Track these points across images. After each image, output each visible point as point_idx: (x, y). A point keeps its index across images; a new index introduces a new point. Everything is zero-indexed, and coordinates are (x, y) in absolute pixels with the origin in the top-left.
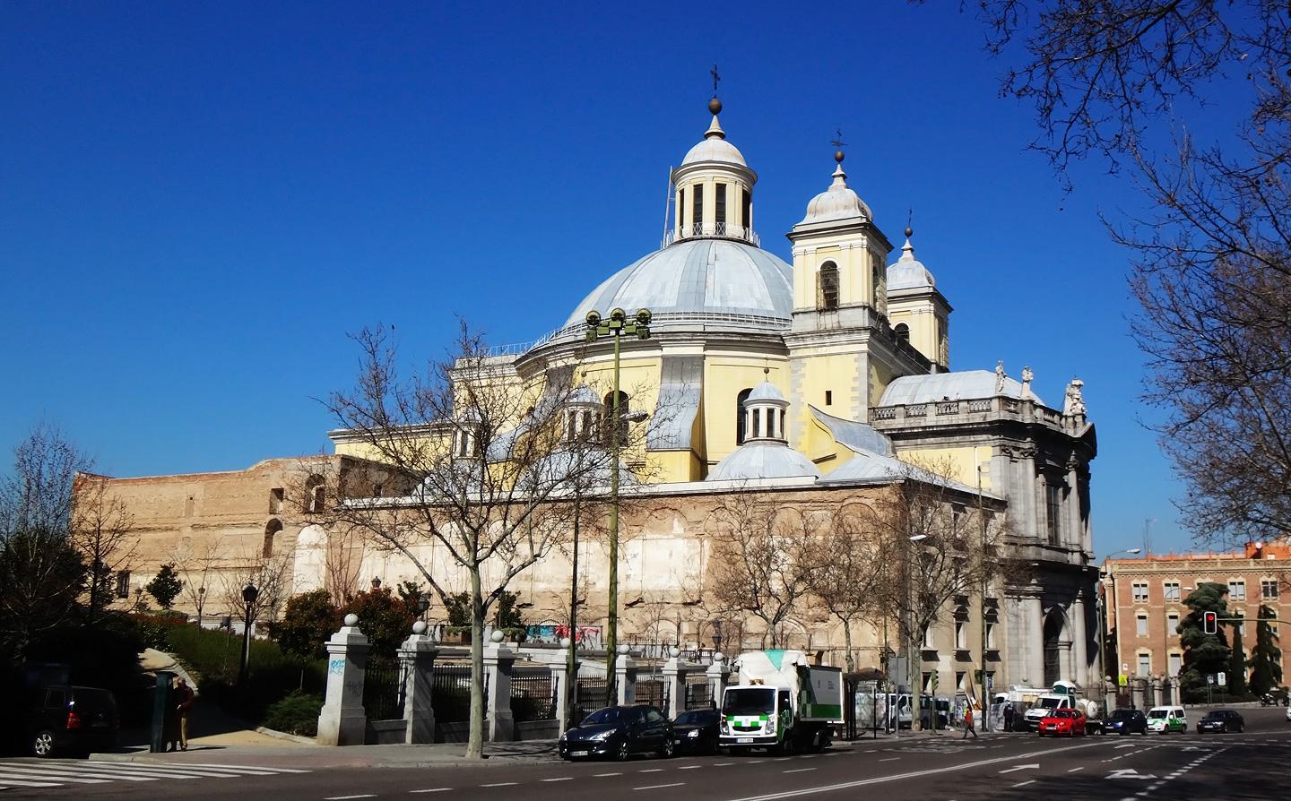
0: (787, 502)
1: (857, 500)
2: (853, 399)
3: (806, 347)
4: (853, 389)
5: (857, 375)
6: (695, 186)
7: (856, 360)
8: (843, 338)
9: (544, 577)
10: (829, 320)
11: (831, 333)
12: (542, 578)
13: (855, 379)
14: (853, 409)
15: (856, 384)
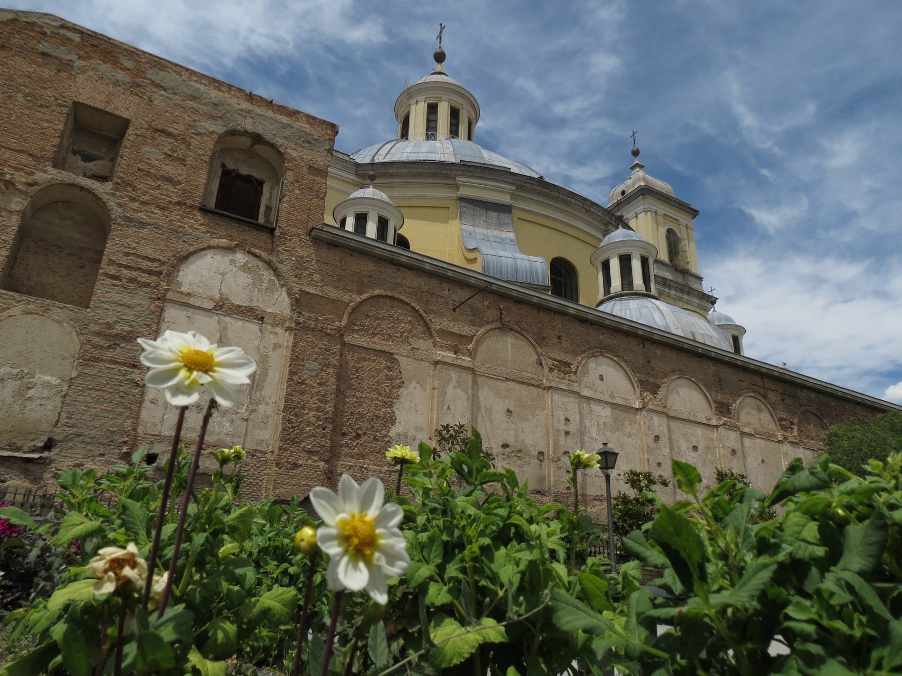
8: (696, 301)
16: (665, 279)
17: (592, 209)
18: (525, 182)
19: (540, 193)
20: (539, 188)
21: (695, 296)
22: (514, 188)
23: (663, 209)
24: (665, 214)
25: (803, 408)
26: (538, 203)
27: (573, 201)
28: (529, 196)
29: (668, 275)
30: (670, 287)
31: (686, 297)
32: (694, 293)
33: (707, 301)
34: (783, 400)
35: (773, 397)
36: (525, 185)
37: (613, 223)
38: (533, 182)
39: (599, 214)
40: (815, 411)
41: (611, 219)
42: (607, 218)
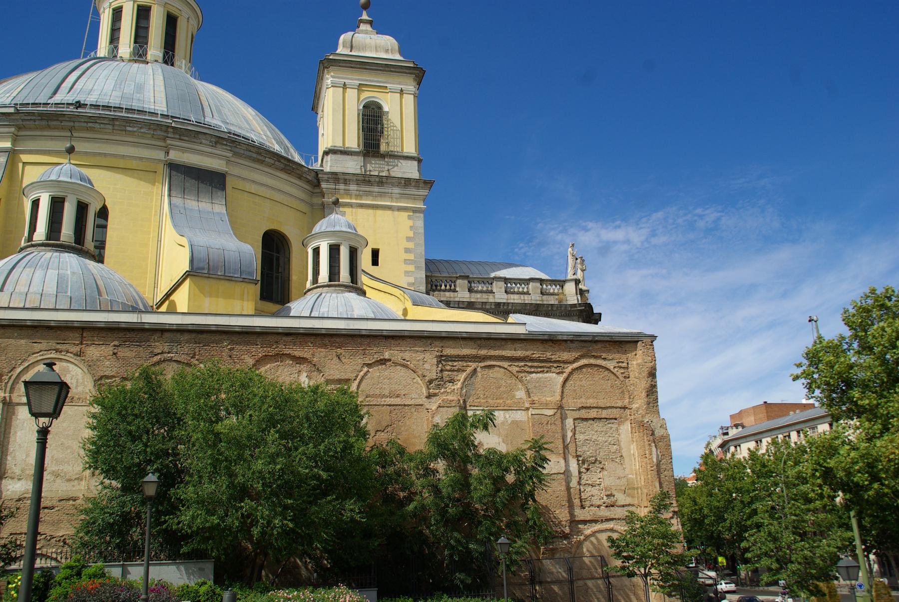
0: (490, 358)
1: (593, 361)
2: (406, 261)
3: (348, 193)
4: (407, 250)
5: (411, 234)
6: (139, 6)
7: (409, 217)
8: (396, 190)
9: (23, 471)
10: (376, 167)
11: (382, 181)
12: (17, 471)
13: (409, 239)
14: (407, 273)
15: (411, 245)
16: (335, 174)
17: (129, 129)
18: (23, 120)
19: (49, 127)
20: (44, 123)
21: (393, 185)
22: (13, 130)
23: (353, 78)
24: (360, 84)
25: (159, 357)
26: (52, 138)
27: (97, 126)
28: (39, 133)
29: (352, 165)
30: (346, 182)
31: (376, 189)
32: (389, 181)
33: (417, 187)
34: (115, 354)
35: (93, 352)
36: (24, 123)
37: (169, 135)
38: (34, 118)
39: (142, 131)
40: (183, 358)
41: (166, 131)
42: (159, 133)
